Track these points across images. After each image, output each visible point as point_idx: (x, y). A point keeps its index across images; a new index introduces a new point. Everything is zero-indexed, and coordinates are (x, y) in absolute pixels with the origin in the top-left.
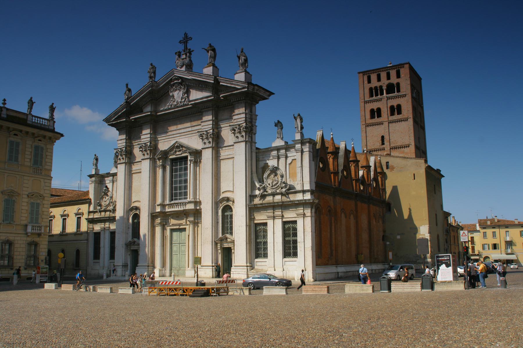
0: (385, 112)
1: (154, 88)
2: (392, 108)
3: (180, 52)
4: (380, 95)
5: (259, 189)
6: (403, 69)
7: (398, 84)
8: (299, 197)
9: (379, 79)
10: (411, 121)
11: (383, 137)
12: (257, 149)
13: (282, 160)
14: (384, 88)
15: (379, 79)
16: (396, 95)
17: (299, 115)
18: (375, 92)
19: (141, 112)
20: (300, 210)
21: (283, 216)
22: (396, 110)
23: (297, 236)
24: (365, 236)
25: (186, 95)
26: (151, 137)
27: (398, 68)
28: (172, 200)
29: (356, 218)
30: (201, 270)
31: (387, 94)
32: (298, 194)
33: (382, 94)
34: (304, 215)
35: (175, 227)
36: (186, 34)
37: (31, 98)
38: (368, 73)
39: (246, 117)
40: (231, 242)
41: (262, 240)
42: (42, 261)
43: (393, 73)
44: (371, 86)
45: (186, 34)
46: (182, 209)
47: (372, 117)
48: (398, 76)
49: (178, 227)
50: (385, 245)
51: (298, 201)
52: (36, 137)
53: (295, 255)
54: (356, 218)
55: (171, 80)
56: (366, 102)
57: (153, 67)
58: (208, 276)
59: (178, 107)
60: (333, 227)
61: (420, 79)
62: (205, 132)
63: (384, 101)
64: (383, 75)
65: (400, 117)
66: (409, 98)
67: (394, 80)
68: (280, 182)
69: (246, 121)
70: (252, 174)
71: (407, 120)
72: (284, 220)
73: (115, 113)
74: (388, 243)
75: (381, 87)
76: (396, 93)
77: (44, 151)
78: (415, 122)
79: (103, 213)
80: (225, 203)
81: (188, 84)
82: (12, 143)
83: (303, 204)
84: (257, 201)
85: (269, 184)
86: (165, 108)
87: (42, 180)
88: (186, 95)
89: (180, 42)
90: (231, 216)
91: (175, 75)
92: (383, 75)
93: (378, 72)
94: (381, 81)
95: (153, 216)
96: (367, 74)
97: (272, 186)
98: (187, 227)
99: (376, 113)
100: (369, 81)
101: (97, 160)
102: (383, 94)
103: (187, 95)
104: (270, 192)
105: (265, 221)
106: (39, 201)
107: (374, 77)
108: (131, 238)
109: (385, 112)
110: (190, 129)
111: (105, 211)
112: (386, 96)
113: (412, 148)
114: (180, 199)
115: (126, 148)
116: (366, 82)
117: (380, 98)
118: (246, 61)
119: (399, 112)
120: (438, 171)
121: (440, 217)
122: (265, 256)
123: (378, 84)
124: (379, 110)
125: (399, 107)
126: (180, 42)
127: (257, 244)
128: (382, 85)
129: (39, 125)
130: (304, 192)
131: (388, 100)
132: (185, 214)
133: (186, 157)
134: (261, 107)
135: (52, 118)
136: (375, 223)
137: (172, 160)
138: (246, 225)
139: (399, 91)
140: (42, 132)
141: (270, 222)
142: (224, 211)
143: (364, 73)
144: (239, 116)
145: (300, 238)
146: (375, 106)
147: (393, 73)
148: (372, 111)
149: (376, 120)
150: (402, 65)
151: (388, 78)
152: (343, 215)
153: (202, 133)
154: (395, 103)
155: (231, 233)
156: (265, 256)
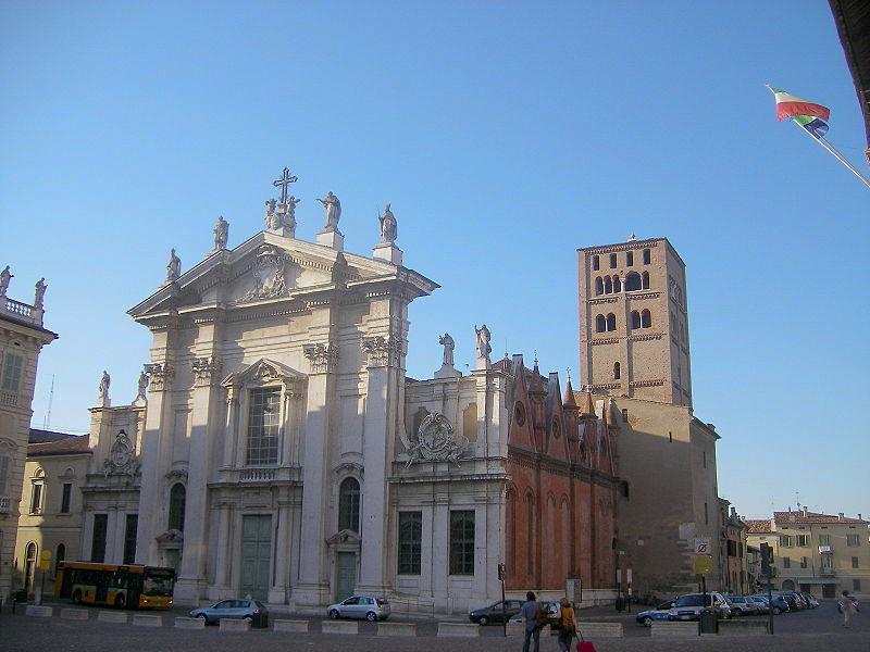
1: (226, 262)
3: (274, 202)
5: (410, 453)
6: (655, 249)
7: (646, 275)
8: (481, 469)
9: (614, 265)
10: (667, 339)
11: (617, 365)
12: (407, 380)
13: (451, 403)
14: (622, 280)
15: (614, 265)
17: (484, 327)
18: (608, 285)
19: (198, 302)
20: (483, 491)
21: (449, 503)
22: (640, 320)
23: (473, 537)
24: (584, 540)
26: (214, 349)
27: (647, 247)
28: (248, 463)
29: (572, 506)
30: (298, 591)
32: (477, 465)
33: (618, 290)
34: (488, 503)
35: (251, 512)
36: (286, 172)
37: (8, 268)
39: (391, 326)
40: (354, 543)
41: (411, 543)
45: (286, 172)
46: (267, 480)
47: (601, 329)
48: (647, 260)
49: (257, 513)
50: (617, 556)
51: (478, 475)
52: (11, 338)
53: (469, 570)
54: (572, 506)
55: (257, 251)
57: (224, 226)
58: (311, 602)
59: (269, 299)
60: (534, 523)
61: (682, 265)
63: (622, 303)
64: (621, 257)
65: (646, 331)
66: (664, 298)
67: (639, 267)
69: (390, 331)
70: (397, 425)
72: (452, 508)
73: (151, 301)
74: (622, 553)
75: (617, 278)
77: (23, 364)
78: (674, 341)
79: (115, 481)
80: (345, 474)
82: (10, 356)
83: (490, 480)
84: (405, 473)
86: (244, 300)
87: (15, 416)
90: (357, 498)
92: (621, 257)
93: (612, 251)
95: (212, 489)
96: (592, 256)
97: (434, 448)
98: (275, 513)
100: (597, 267)
101: (107, 380)
104: (428, 457)
105: (417, 509)
106: (8, 455)
107: (605, 260)
108: (166, 528)
110: (286, 339)
111: (119, 475)
113: (668, 385)
114: (262, 462)
115: (166, 364)
118: (394, 227)
119: (647, 324)
120: (710, 428)
121: (713, 509)
122: (417, 570)
123: (612, 272)
124: (612, 317)
125: (647, 313)
127: (403, 549)
129: (17, 317)
132: (273, 488)
133: (280, 388)
134: (416, 309)
135: (38, 306)
136: (600, 515)
137: (252, 391)
138: (385, 515)
139: (647, 286)
140: (21, 330)
141: (427, 513)
142: (343, 486)
144: (379, 323)
145: (477, 543)
146: (604, 310)
147: (638, 255)
149: (607, 335)
150: (653, 242)
151: (630, 263)
152: (550, 503)
155: (356, 529)
156: (417, 570)
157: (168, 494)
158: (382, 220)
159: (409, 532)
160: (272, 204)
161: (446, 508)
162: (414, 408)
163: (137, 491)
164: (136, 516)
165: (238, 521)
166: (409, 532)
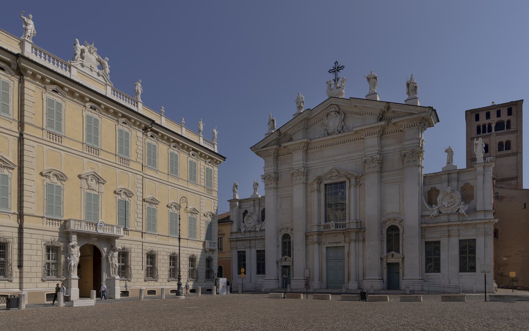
4: (488, 132)
14: (493, 126)
16: (506, 132)
25: (343, 123)
31: (495, 130)
33: (490, 130)
38: (477, 111)
42: (216, 274)
44: (478, 124)
62: (369, 158)
68: (457, 204)
71: (517, 154)
75: (490, 125)
76: (506, 130)
81: (345, 112)
85: (444, 206)
88: (343, 123)
91: (332, 103)
94: (491, 118)
100: (477, 118)
102: (491, 131)
103: (344, 123)
107: (482, 116)
112: (496, 133)
116: (474, 120)
117: (488, 134)
123: (487, 122)
128: (492, 123)
131: (497, 136)
143: (472, 111)
153: (367, 158)
154: (504, 139)
161: (457, 238)
162: (428, 188)
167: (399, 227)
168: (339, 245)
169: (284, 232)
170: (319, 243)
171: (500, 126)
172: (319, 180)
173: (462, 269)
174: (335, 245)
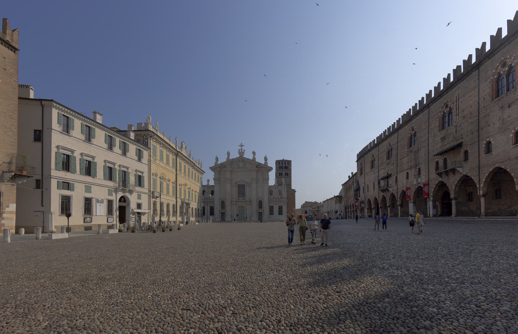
0: (284, 174)
2: (286, 173)
7: (288, 167)
9: (282, 164)
14: (284, 167)
15: (282, 164)
28: (238, 197)
33: (283, 168)
43: (287, 163)
47: (280, 175)
48: (288, 164)
56: (278, 170)
64: (284, 163)
65: (288, 176)
67: (287, 165)
75: (283, 166)
89: (239, 146)
92: (284, 163)
99: (281, 174)
100: (279, 164)
107: (281, 163)
109: (284, 174)
119: (288, 175)
123: (282, 165)
125: (288, 173)
126: (239, 146)
130: (285, 198)
137: (238, 185)
139: (288, 168)
142: (259, 202)
146: (281, 172)
147: (287, 163)
148: (280, 173)
151: (285, 164)
154: (287, 172)
157: (220, 203)
158: (265, 158)
159: (271, 209)
160: (239, 150)
163: (213, 202)
164: (213, 207)
165: (238, 207)
166: (271, 209)
167: (262, 201)
168: (243, 206)
169: (222, 200)
170: (236, 205)
171: (285, 167)
172: (236, 183)
173: (279, 214)
174: (242, 206)
